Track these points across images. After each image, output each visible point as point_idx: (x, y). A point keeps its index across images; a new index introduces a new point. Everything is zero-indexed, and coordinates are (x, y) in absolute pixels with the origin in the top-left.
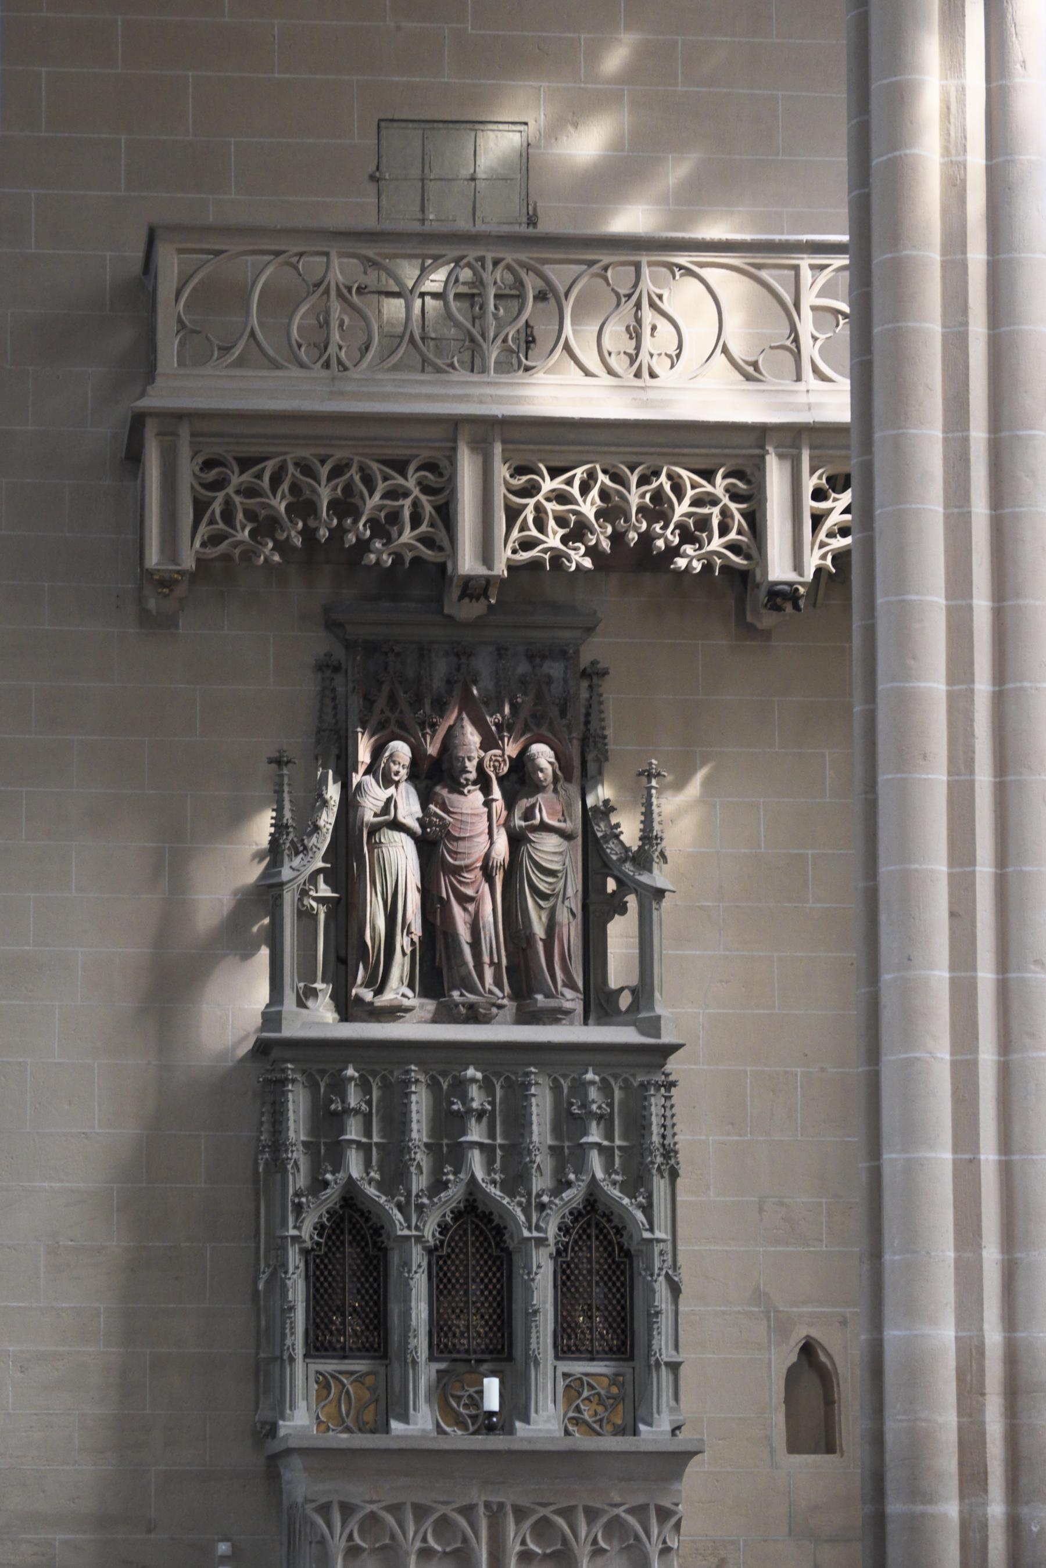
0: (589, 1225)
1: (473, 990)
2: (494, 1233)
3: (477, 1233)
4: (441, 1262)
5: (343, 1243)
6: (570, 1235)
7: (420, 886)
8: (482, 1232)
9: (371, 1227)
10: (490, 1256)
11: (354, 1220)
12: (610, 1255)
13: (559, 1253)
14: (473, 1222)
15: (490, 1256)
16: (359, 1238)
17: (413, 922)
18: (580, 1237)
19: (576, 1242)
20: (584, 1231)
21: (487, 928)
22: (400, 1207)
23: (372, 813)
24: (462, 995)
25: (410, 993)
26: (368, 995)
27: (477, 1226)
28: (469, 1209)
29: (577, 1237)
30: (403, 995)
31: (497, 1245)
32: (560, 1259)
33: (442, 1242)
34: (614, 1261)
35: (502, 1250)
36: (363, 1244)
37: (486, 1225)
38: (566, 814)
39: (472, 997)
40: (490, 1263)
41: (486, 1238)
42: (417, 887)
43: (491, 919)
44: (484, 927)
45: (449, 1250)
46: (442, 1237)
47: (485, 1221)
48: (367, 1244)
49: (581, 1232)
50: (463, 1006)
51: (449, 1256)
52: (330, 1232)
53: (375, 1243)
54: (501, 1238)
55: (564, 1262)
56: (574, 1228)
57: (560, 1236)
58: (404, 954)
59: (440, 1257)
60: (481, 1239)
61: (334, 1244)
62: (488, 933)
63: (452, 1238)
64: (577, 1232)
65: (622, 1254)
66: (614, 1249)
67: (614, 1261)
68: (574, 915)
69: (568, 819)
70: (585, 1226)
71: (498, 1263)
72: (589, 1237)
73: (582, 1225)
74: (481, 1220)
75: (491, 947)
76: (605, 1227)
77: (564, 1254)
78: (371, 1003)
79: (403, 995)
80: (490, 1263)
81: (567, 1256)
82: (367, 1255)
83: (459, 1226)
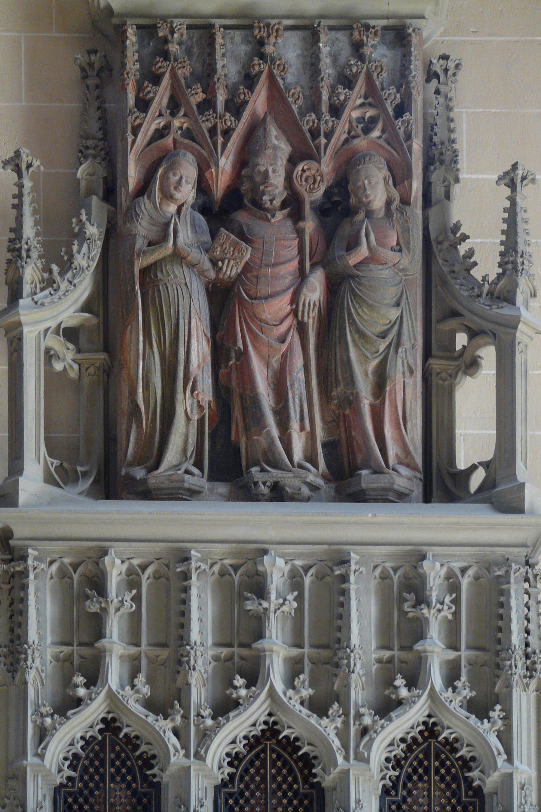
0: (427, 756)
1: (276, 465)
2: (300, 764)
3: (279, 764)
4: (231, 802)
5: (103, 778)
6: (401, 768)
7: (209, 335)
8: (285, 764)
9: (140, 756)
10: (296, 794)
11: (118, 748)
12: (454, 794)
13: (386, 791)
14: (273, 751)
15: (296, 794)
16: (124, 770)
17: (199, 379)
18: (415, 771)
19: (409, 778)
20: (421, 763)
21: (296, 386)
22: (176, 732)
23: (146, 242)
24: (263, 470)
25: (196, 471)
26: (139, 473)
27: (279, 757)
28: (268, 734)
29: (410, 770)
30: (187, 472)
31: (306, 780)
32: (387, 798)
33: (232, 776)
34: (459, 802)
35: (313, 786)
36: (129, 778)
37: (291, 755)
38: (401, 242)
39: (275, 474)
40: (295, 802)
41: (291, 771)
42: (206, 336)
43: (301, 376)
44: (292, 385)
45: (242, 786)
46: (233, 770)
47: (289, 749)
48: (134, 779)
49: (415, 763)
50: (264, 483)
51: (242, 794)
52: (87, 763)
53: (145, 778)
54: (310, 771)
55: (394, 802)
56: (406, 758)
57: (387, 768)
58: (188, 419)
59: (231, 795)
60: (284, 771)
61: (92, 778)
62: (296, 392)
63: (246, 770)
64: (411, 765)
65: (470, 793)
66: (459, 787)
67: (459, 802)
68: (411, 372)
69: (404, 250)
70: (421, 756)
71: (306, 802)
72: (427, 771)
73: (417, 756)
74: (285, 750)
75: (302, 412)
76: (448, 758)
77: (393, 793)
78: (144, 481)
79: (187, 472)
80: (295, 802)
81: (397, 795)
82: (135, 793)
83: (257, 756)
